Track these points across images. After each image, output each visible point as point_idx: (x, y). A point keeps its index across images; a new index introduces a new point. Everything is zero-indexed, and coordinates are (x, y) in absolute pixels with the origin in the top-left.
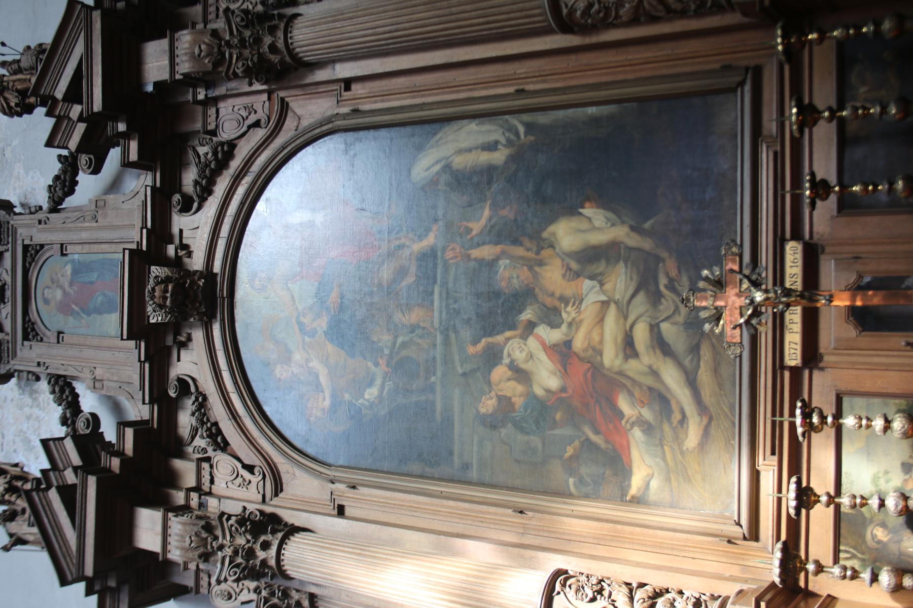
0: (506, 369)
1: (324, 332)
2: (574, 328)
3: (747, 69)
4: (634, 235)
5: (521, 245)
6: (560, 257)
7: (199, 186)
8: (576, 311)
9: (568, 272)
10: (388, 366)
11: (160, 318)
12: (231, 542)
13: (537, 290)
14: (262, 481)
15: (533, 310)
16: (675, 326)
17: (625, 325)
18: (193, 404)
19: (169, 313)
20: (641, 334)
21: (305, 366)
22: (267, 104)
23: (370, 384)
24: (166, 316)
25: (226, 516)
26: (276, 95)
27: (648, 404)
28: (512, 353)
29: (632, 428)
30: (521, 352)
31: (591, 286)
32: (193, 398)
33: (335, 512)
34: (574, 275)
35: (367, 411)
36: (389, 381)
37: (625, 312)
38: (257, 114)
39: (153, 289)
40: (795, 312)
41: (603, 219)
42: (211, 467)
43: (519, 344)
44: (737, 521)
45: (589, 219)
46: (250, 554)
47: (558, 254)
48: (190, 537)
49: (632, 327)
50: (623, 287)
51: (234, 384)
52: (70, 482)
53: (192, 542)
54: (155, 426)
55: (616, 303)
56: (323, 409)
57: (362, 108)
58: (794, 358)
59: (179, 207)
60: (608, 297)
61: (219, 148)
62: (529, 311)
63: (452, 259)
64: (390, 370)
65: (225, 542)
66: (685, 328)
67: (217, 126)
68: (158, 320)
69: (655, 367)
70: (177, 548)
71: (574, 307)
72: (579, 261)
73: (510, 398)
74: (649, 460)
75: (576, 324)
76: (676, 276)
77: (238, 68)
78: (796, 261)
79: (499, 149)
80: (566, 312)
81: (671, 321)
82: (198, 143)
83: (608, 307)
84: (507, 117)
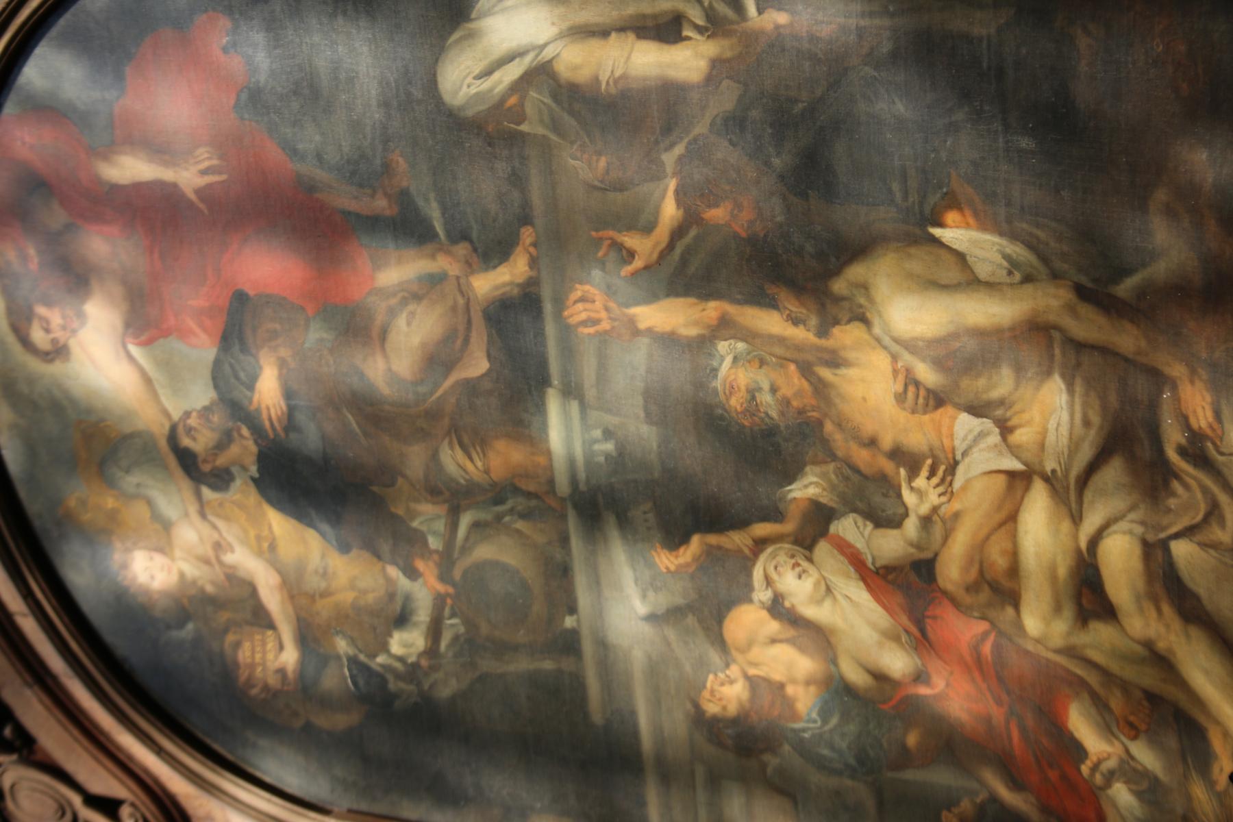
0: (764, 614)
1: (253, 479)
2: (938, 530)
4: (1086, 310)
5: (773, 304)
6: (885, 348)
8: (941, 489)
9: (911, 389)
10: (444, 577)
13: (829, 427)
15: (824, 476)
16: (1212, 552)
17: (1076, 537)
21: (213, 560)
23: (402, 620)
27: (1147, 731)
28: (774, 576)
30: (800, 577)
31: (975, 433)
34: (927, 399)
35: (402, 685)
36: (453, 615)
37: (1074, 505)
41: (999, 259)
43: (793, 556)
45: (960, 257)
47: (878, 340)
49: (1094, 542)
50: (1064, 441)
55: (1047, 479)
56: (282, 671)
60: (1025, 464)
62: (815, 479)
63: (584, 323)
64: (451, 590)
69: (1161, 645)
71: (935, 480)
72: (939, 364)
73: (781, 686)
75: (944, 521)
76: (1211, 426)
79: (688, 38)
80: (912, 489)
81: (1199, 537)
83: (1027, 488)
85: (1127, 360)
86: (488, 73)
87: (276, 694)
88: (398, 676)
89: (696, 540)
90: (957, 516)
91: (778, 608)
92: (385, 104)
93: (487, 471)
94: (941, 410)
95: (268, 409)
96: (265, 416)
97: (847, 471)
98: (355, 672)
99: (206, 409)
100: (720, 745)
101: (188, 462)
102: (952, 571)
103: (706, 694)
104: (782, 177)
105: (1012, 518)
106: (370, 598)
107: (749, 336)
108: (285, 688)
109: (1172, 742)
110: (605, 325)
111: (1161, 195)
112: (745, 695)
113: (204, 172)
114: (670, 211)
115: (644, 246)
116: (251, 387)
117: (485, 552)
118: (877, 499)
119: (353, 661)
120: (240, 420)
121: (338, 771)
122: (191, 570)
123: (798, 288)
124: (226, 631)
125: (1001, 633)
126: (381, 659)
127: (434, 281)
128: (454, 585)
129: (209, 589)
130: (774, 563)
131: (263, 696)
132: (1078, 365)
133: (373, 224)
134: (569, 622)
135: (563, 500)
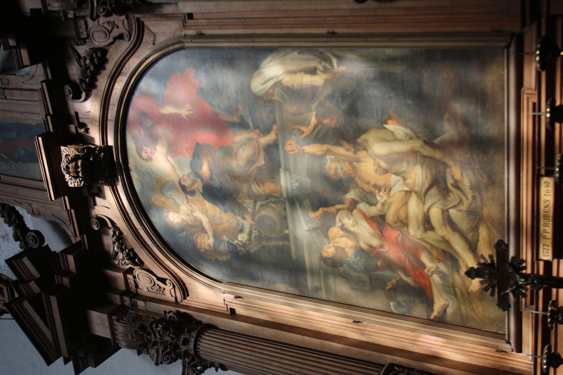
0: (339, 229)
1: (201, 193)
2: (386, 206)
3: (513, 35)
4: (427, 147)
6: (372, 157)
7: (84, 83)
8: (387, 195)
9: (379, 169)
10: (253, 219)
11: (76, 184)
12: (161, 340)
13: (357, 179)
14: (173, 289)
17: (423, 209)
18: (113, 237)
19: (82, 181)
20: (435, 214)
22: (126, 22)
23: (241, 231)
24: (81, 182)
25: (154, 325)
26: (132, 16)
29: (432, 275)
32: (111, 232)
33: (229, 312)
35: (241, 248)
36: (255, 230)
38: (119, 29)
39: (67, 167)
40: (547, 225)
42: (134, 277)
43: (347, 214)
44: (507, 340)
45: (392, 133)
46: (176, 347)
47: (370, 155)
48: (131, 335)
49: (429, 210)
51: (141, 225)
52: (36, 292)
53: (133, 337)
54: (87, 248)
55: (416, 193)
56: (209, 245)
57: (204, 32)
58: (546, 255)
59: (71, 96)
61: (94, 55)
63: (291, 151)
64: (254, 223)
65: (157, 340)
66: (467, 214)
67: (88, 35)
68: (75, 185)
69: (446, 238)
70: (123, 341)
71: (386, 193)
72: (386, 162)
73: (344, 249)
74: (444, 295)
77: (100, 12)
78: (549, 191)
80: (379, 196)
81: (458, 208)
82: (75, 44)
84: (321, 49)
85: (437, 161)
86: (264, 83)
87: (208, 251)
88: (240, 246)
89: (321, 210)
90: (391, 203)
91: (343, 228)
92: (237, 92)
93: (264, 191)
94: (387, 174)
95: (205, 174)
96: (204, 176)
97: (362, 191)
98: (229, 245)
99: (189, 174)
100: (327, 265)
101: (184, 188)
102: (390, 218)
103: (323, 251)
104: (344, 111)
105: (406, 203)
106: (233, 225)
107: (335, 154)
108: (210, 249)
109: (449, 263)
110: (296, 151)
111: (446, 116)
112: (334, 251)
113: (188, 111)
114: (313, 120)
115: (307, 130)
116: (201, 168)
117: (264, 213)
118: (370, 198)
119: (228, 242)
120: (198, 177)
121: (224, 271)
122: (185, 217)
123: (348, 141)
124: (194, 234)
125: (403, 235)
126: (236, 241)
127: (250, 139)
128: (255, 221)
129: (190, 223)
130: (342, 216)
131: (204, 251)
132: (424, 162)
133: (233, 125)
134: (286, 232)
135: (285, 199)
